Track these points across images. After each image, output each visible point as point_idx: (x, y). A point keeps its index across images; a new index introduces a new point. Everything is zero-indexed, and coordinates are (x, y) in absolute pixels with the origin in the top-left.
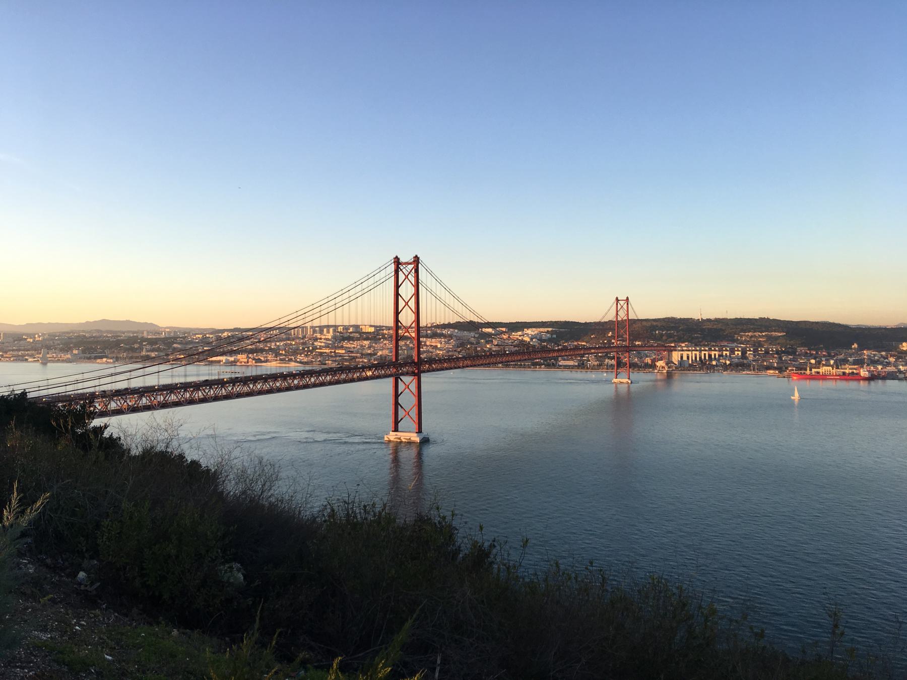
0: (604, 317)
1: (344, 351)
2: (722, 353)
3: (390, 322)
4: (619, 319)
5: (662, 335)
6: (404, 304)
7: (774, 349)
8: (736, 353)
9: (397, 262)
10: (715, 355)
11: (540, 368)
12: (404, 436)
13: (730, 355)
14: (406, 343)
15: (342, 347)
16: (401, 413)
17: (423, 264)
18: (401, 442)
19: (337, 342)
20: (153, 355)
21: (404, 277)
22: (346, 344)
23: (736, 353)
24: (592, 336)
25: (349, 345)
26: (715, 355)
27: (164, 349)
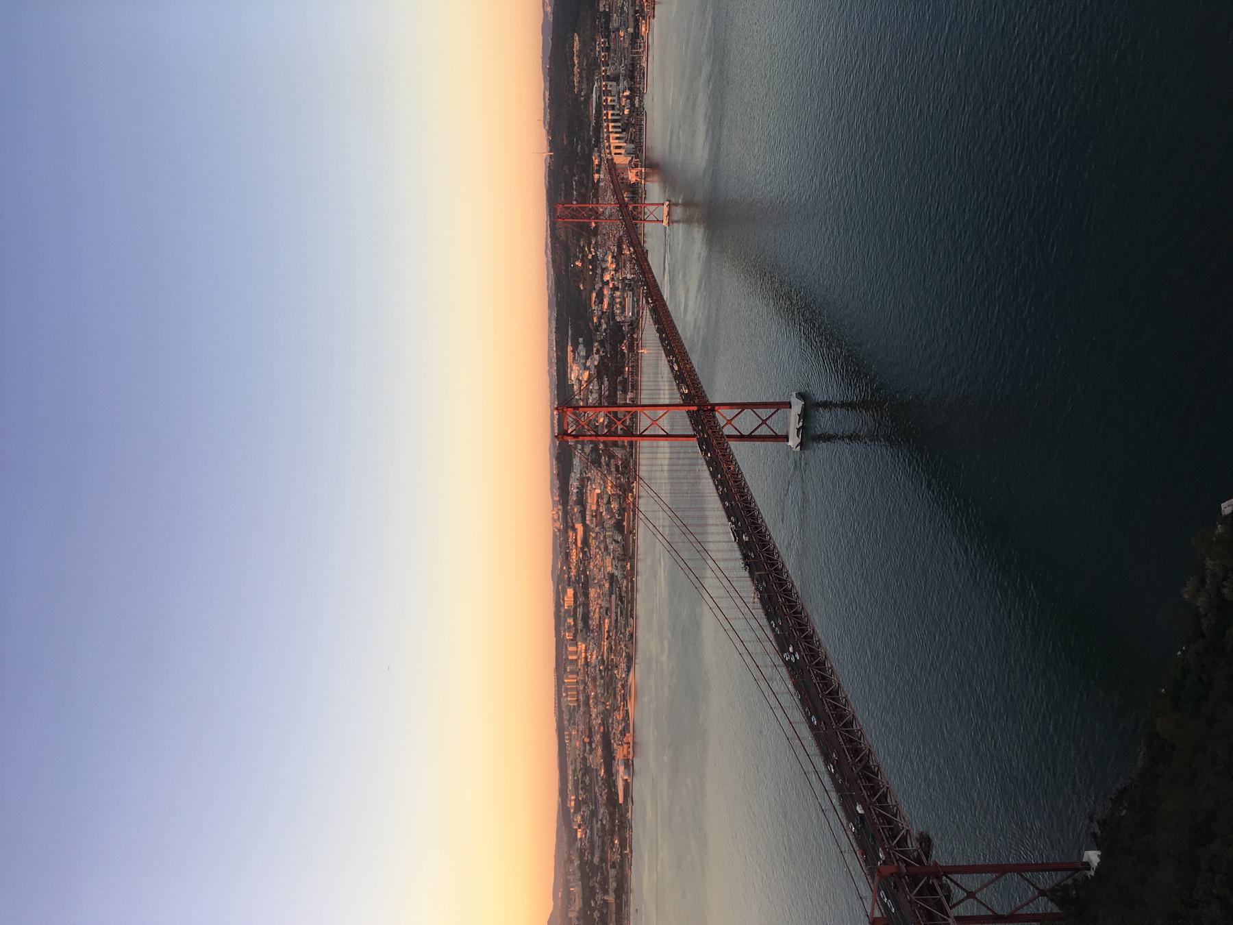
1: (607, 621)
5: (579, 194)
7: (602, 40)
11: (637, 339)
12: (794, 423)
13: (611, 96)
14: (594, 538)
15: (600, 626)
18: (802, 427)
19: (592, 635)
20: (613, 885)
22: (593, 623)
23: (609, 88)
24: (582, 288)
25: (597, 616)
27: (602, 874)
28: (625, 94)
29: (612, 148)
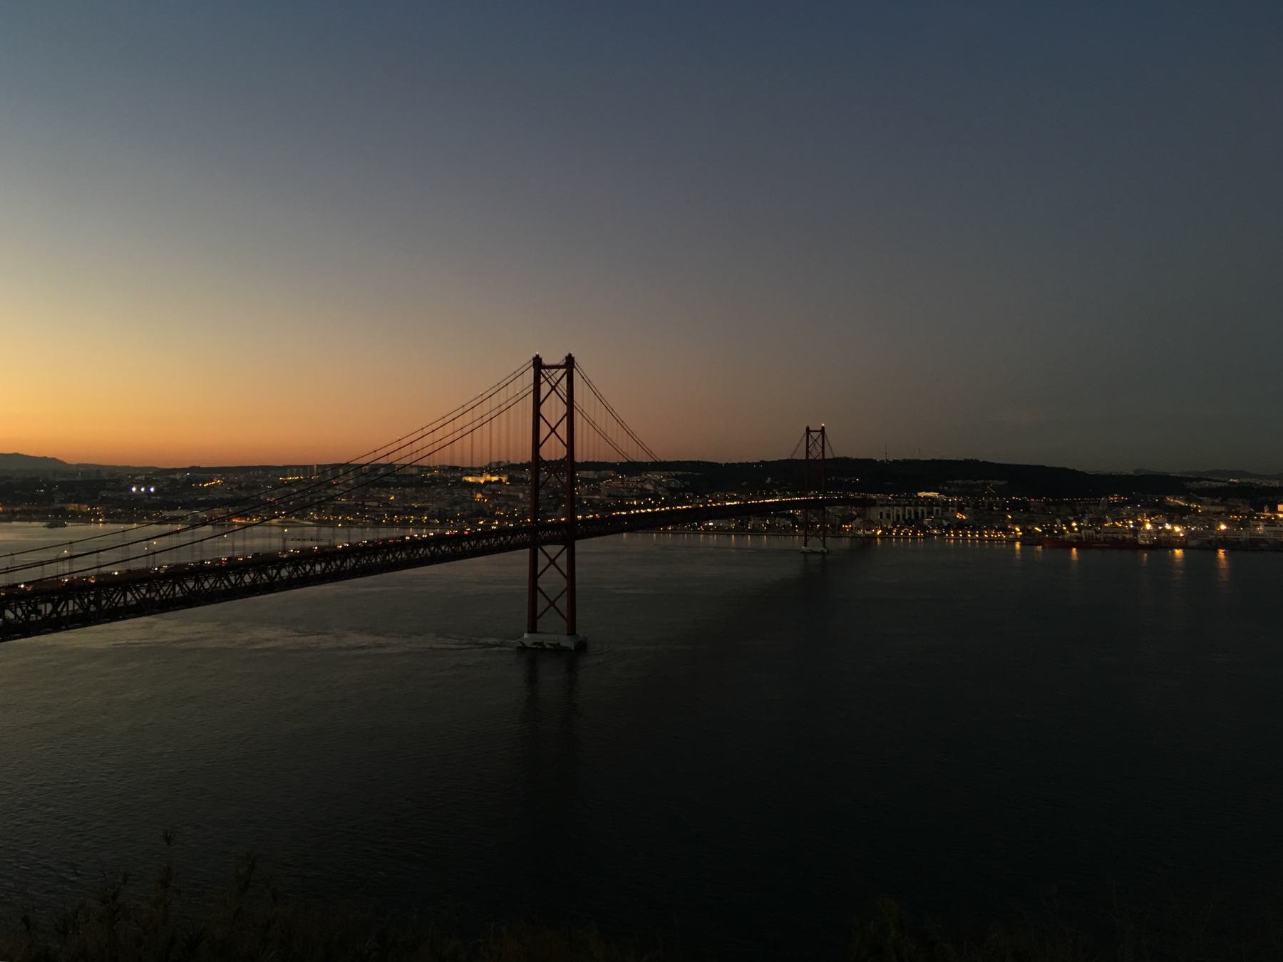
0: (792, 456)
2: (933, 509)
3: (528, 457)
4: (810, 457)
6: (549, 430)
8: (950, 508)
9: (537, 363)
10: (923, 513)
12: (548, 639)
13: (943, 511)
16: (542, 604)
17: (579, 370)
18: (544, 649)
21: (550, 388)
23: (950, 508)
24: (744, 484)
26: (923, 513)
28: (944, 521)
29: (887, 508)
